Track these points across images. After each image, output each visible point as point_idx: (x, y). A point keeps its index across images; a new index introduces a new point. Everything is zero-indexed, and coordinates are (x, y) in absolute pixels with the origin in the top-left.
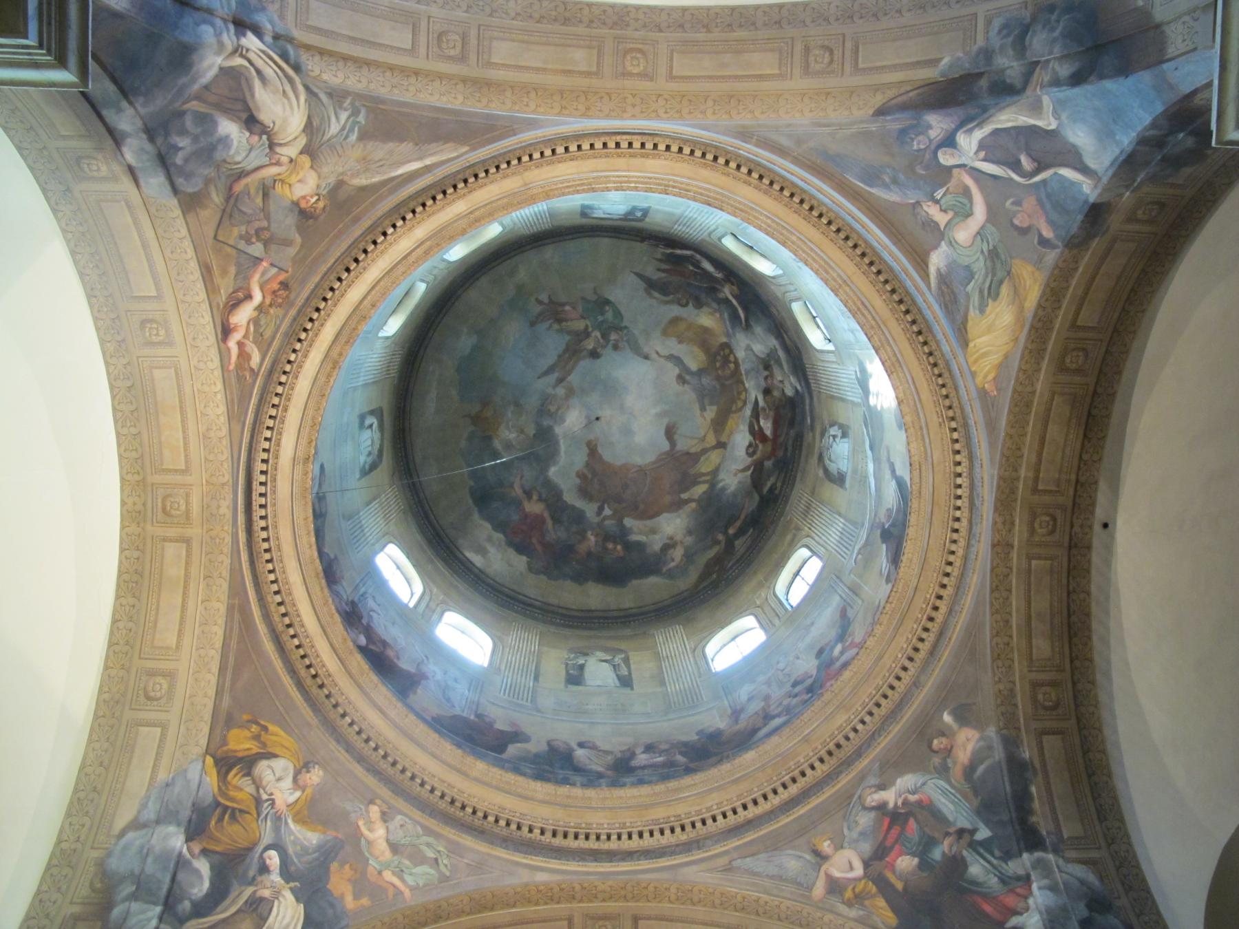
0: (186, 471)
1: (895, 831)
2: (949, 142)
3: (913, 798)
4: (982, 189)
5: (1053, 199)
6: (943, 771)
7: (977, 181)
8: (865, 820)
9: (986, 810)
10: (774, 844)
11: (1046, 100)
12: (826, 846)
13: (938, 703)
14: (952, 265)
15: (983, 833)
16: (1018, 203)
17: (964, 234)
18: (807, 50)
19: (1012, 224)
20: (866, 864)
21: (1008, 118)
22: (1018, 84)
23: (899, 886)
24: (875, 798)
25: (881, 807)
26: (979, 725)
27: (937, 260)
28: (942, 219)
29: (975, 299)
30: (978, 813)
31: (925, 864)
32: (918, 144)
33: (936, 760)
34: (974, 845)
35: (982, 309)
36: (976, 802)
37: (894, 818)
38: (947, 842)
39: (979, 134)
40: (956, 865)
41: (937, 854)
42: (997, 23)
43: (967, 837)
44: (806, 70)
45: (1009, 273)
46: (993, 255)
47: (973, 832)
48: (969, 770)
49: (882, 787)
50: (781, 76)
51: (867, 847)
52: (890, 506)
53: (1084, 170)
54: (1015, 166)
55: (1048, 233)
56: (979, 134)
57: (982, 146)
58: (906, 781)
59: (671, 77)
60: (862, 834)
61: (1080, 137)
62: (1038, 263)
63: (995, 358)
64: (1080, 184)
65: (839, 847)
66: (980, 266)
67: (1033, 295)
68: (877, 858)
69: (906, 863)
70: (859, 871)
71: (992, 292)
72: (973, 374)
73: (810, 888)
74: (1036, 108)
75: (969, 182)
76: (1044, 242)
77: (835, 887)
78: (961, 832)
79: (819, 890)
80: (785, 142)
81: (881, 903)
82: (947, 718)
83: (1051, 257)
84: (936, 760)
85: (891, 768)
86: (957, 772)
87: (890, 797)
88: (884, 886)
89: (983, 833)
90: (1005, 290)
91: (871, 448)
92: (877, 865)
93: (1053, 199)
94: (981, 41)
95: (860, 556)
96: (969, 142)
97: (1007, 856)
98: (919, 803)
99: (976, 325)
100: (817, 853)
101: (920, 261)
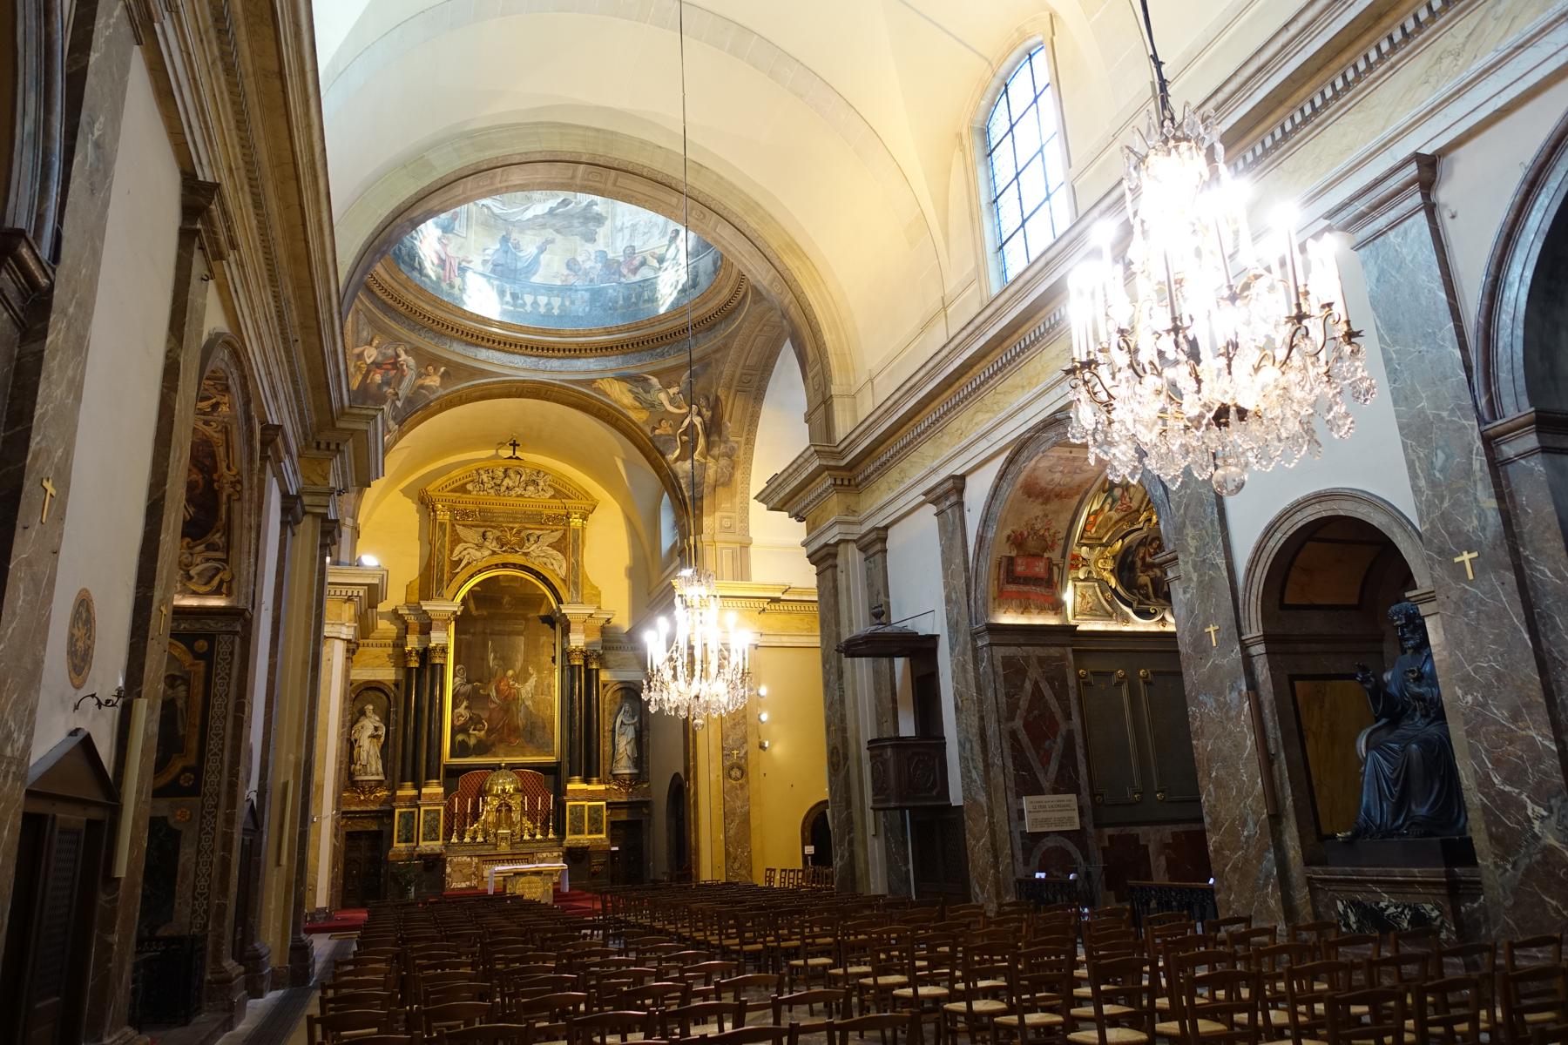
0: (614, 184)
1: (390, 367)
2: (699, 414)
3: (405, 367)
4: (679, 414)
5: (670, 440)
6: (420, 376)
7: (683, 414)
8: (390, 352)
9: (409, 401)
10: (372, 322)
11: (703, 461)
12: (376, 342)
13: (448, 363)
14: (651, 386)
15: (399, 404)
16: (671, 426)
17: (662, 396)
18: (751, 375)
19: (662, 420)
20: (373, 363)
21: (701, 441)
22: (712, 453)
23: (369, 381)
24: (401, 351)
25: (398, 356)
26: (442, 385)
27: (654, 380)
28: (672, 391)
29: (635, 390)
30: (407, 397)
31: (380, 386)
32: (703, 402)
33: (423, 370)
34: (393, 402)
35: (630, 391)
36: (410, 395)
37: (396, 365)
38: (391, 390)
39: (699, 427)
40: (383, 399)
41: (385, 389)
42: (736, 445)
43: (395, 398)
44: (742, 374)
45: (644, 408)
46: (653, 406)
47: (398, 399)
48: (422, 387)
49: (406, 352)
50: (744, 365)
51: (380, 358)
52: (522, 248)
53: (677, 459)
54: (684, 433)
55: (657, 432)
56: (699, 427)
57: (695, 425)
58: (411, 361)
59: (757, 336)
60: (385, 354)
61: (687, 465)
62: (646, 422)
63: (608, 390)
64: (672, 454)
65: (376, 348)
66: (648, 397)
67: (633, 415)
68: (377, 365)
69: (378, 378)
70: (369, 361)
71: (636, 398)
72: (602, 379)
73: (357, 346)
74: (701, 454)
75: (683, 411)
76: (654, 429)
77: (360, 356)
78: (397, 394)
79: (357, 351)
80: (718, 355)
81: (360, 378)
82: (442, 369)
83: (648, 430)
84: (423, 370)
85: (414, 351)
86: (420, 382)
87: (403, 357)
88: (366, 376)
89: (399, 404)
90: (637, 404)
91: (551, 211)
92: (373, 367)
93: (670, 440)
94: (732, 439)
95: (486, 210)
96: (697, 420)
97: (394, 418)
98: (403, 371)
99: (624, 386)
100: (372, 340)
101: (655, 374)
